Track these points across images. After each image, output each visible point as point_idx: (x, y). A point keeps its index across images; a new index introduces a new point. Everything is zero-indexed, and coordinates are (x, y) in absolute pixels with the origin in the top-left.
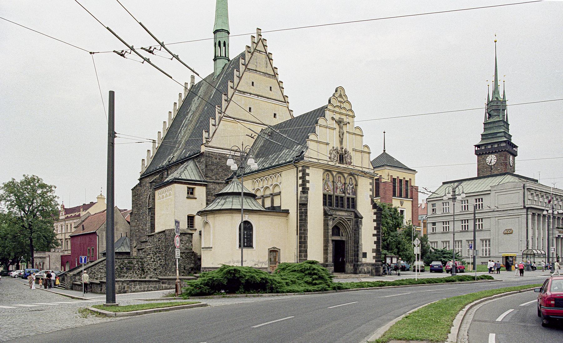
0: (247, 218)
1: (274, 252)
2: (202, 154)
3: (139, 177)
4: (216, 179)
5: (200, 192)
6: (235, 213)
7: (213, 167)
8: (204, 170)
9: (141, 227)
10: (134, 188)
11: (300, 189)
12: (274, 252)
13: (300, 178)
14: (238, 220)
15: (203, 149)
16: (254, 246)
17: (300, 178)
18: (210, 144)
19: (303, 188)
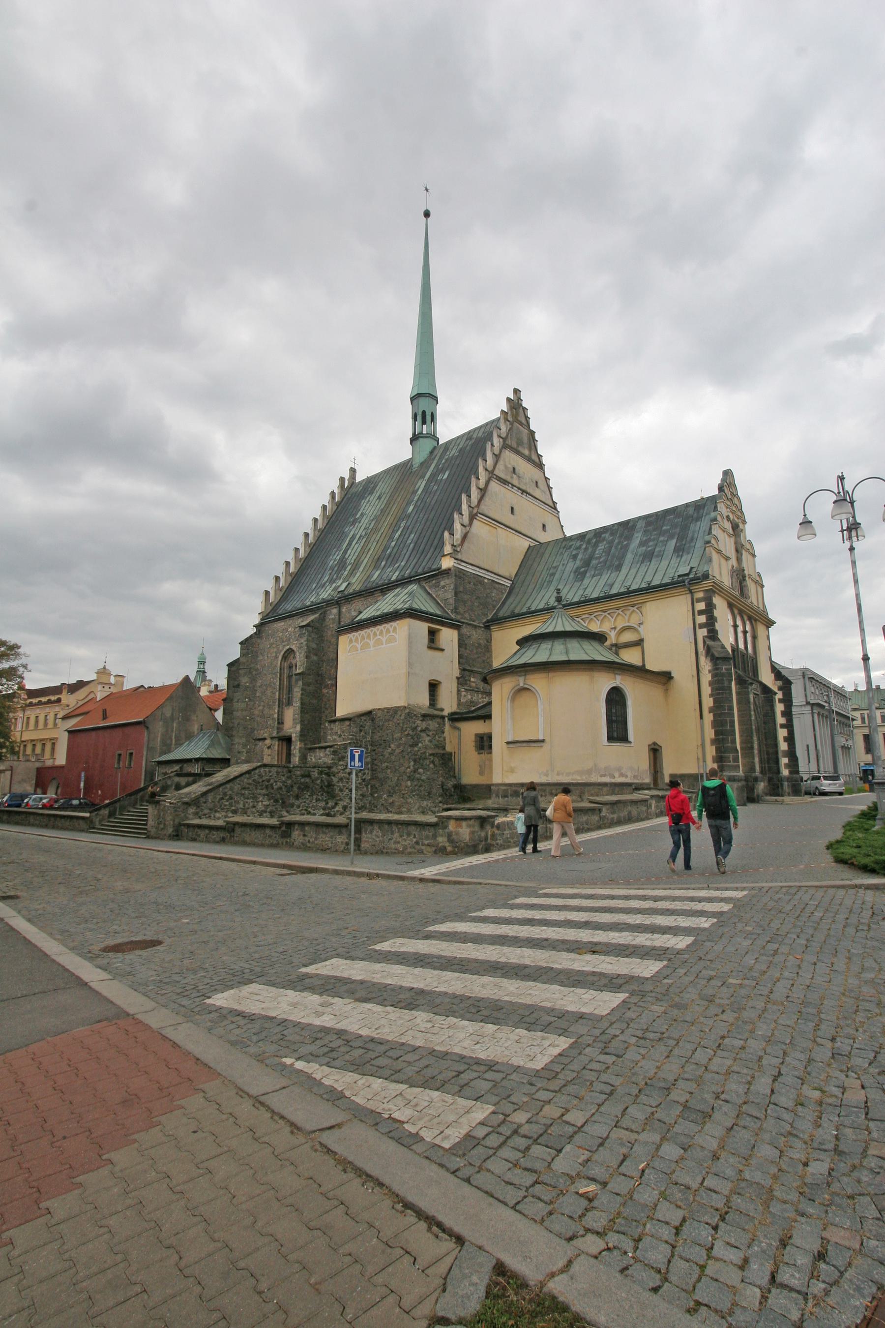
0: (618, 681)
1: (655, 751)
2: (447, 572)
3: (257, 621)
4: (471, 620)
5: (448, 637)
6: (599, 671)
7: (466, 597)
8: (452, 601)
9: (256, 712)
10: (247, 640)
11: (703, 633)
12: (655, 751)
13: (701, 613)
14: (605, 682)
15: (447, 563)
16: (631, 737)
17: (701, 613)
18: (459, 556)
19: (709, 632)
